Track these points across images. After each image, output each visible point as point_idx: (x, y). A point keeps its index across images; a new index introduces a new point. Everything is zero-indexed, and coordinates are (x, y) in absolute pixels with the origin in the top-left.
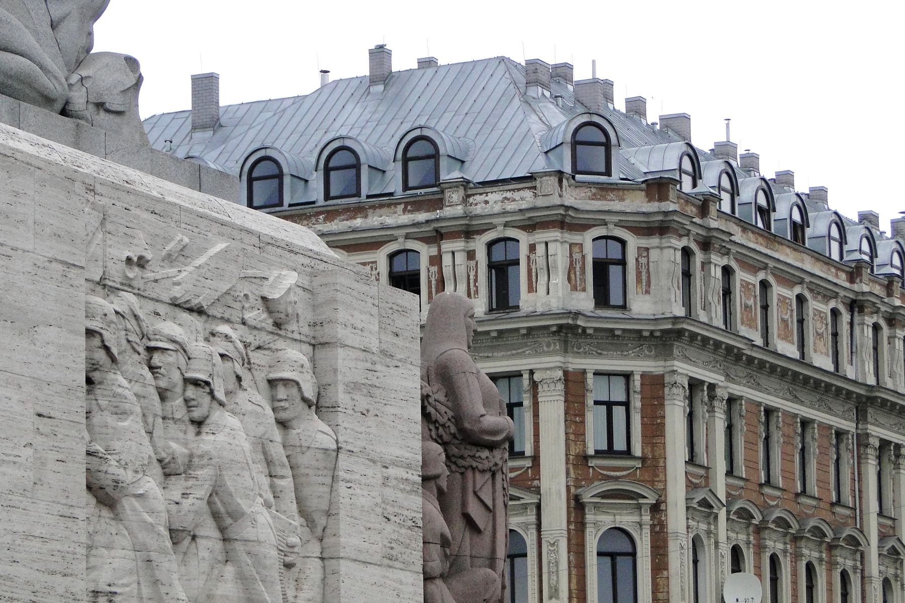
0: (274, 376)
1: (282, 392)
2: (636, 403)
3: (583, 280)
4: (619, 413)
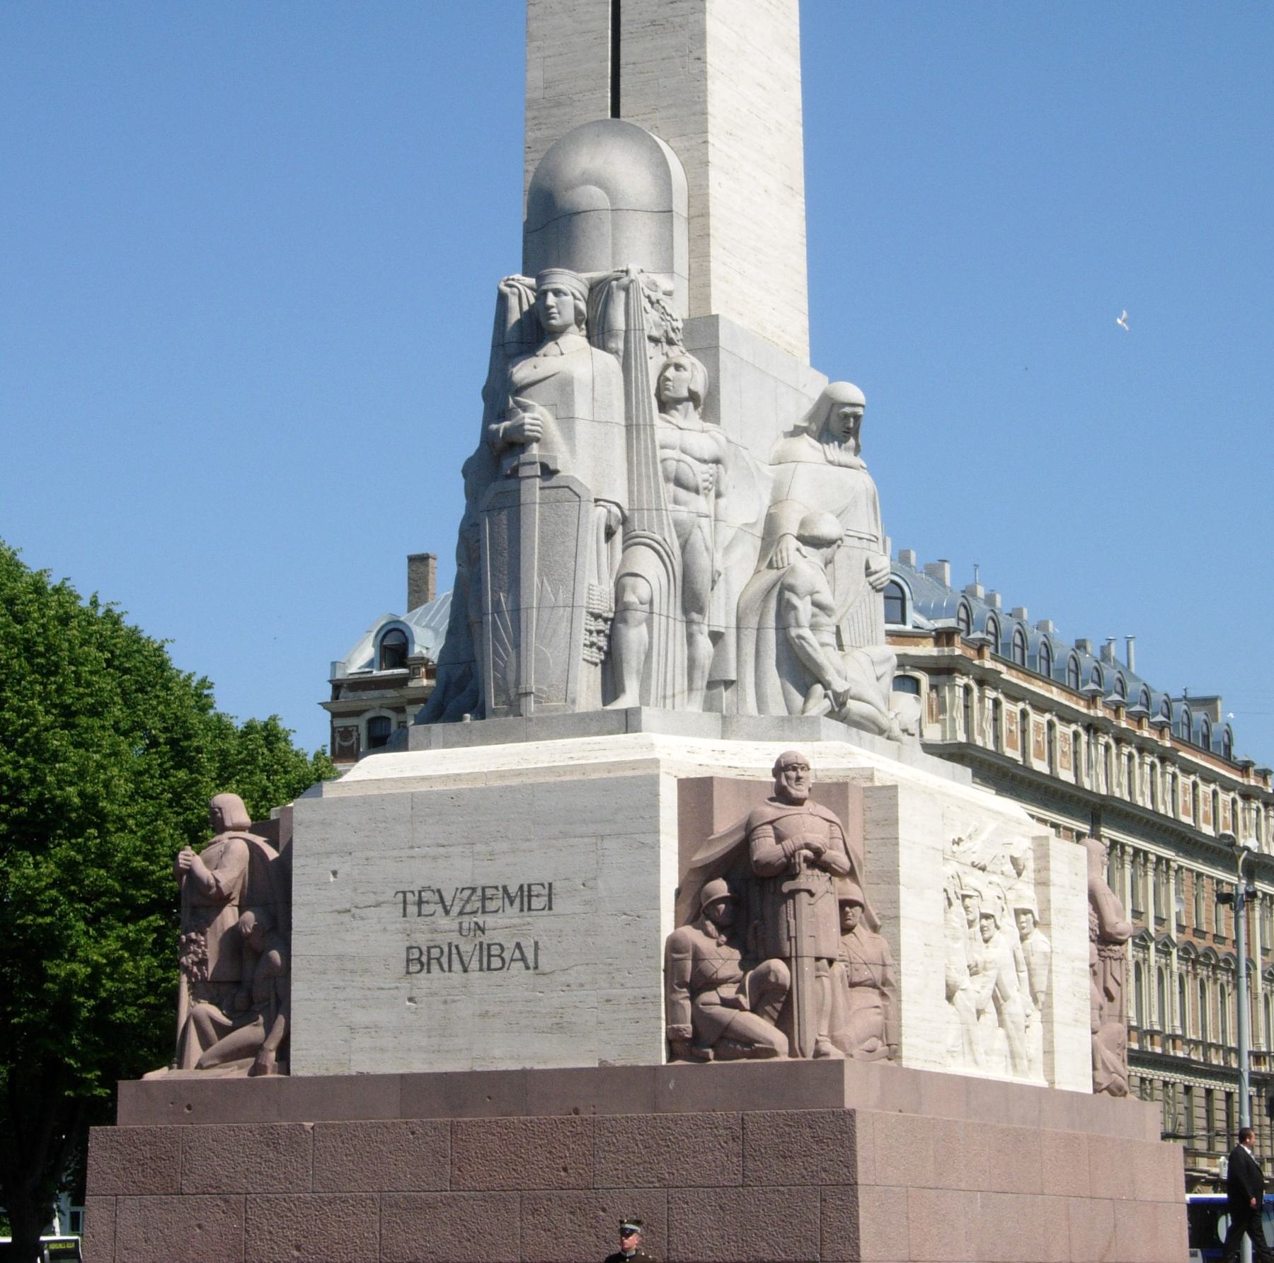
0: (1019, 906)
1: (1023, 918)
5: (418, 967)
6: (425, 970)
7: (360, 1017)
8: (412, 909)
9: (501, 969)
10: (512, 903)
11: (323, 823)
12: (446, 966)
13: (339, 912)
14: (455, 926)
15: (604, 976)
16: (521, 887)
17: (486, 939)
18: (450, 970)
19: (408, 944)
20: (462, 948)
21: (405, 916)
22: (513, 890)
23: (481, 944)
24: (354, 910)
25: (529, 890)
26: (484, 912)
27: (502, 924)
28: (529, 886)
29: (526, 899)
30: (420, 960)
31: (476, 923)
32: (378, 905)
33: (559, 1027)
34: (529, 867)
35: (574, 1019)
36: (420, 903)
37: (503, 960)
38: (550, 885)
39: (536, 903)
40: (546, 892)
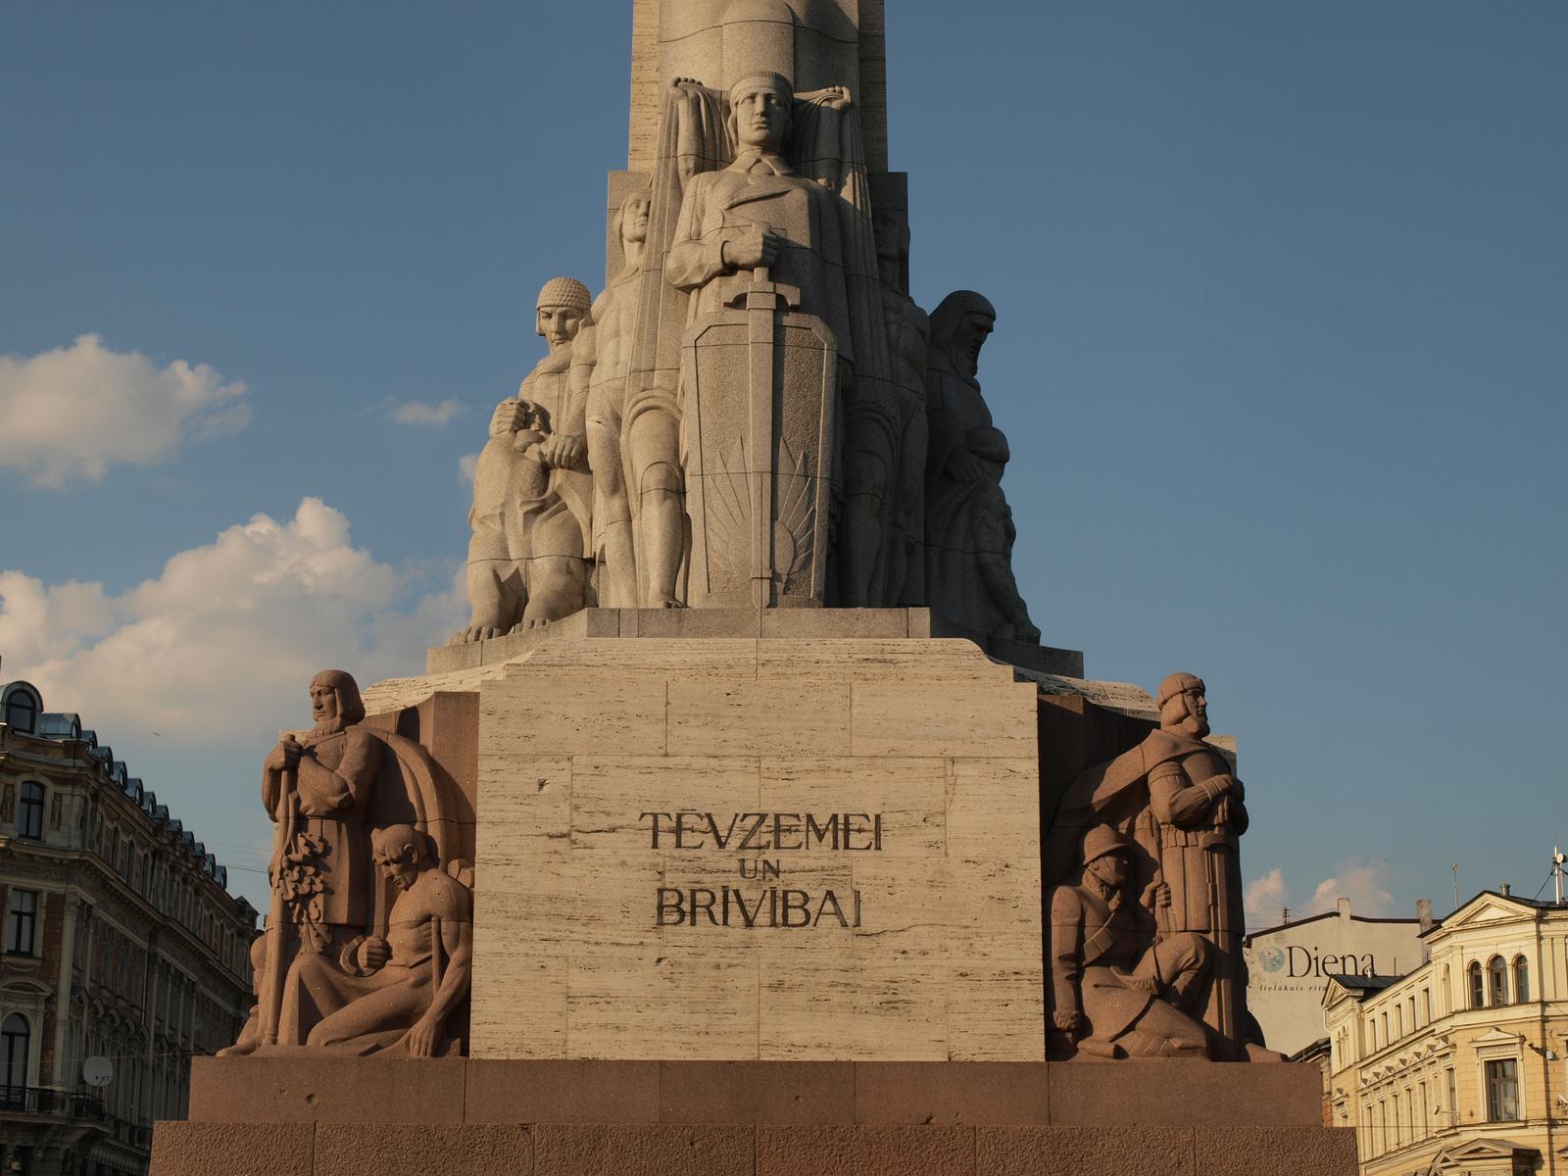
2: (42, 915)
3: (12, 814)
4: (26, 920)
5: (675, 917)
6: (688, 919)
7: (580, 982)
8: (667, 840)
9: (802, 925)
10: (821, 837)
11: (528, 714)
12: (719, 917)
13: (551, 836)
14: (735, 865)
15: (958, 943)
16: (834, 818)
17: (779, 884)
18: (725, 923)
19: (659, 885)
20: (744, 895)
21: (655, 845)
22: (822, 820)
23: (774, 892)
24: (574, 835)
26: (778, 847)
27: (805, 864)
28: (846, 817)
29: (841, 835)
31: (766, 862)
32: (613, 830)
33: (890, 1006)
34: (859, 795)
35: (912, 997)
36: (678, 830)
38: (878, 817)
39: (855, 840)
40: (872, 825)
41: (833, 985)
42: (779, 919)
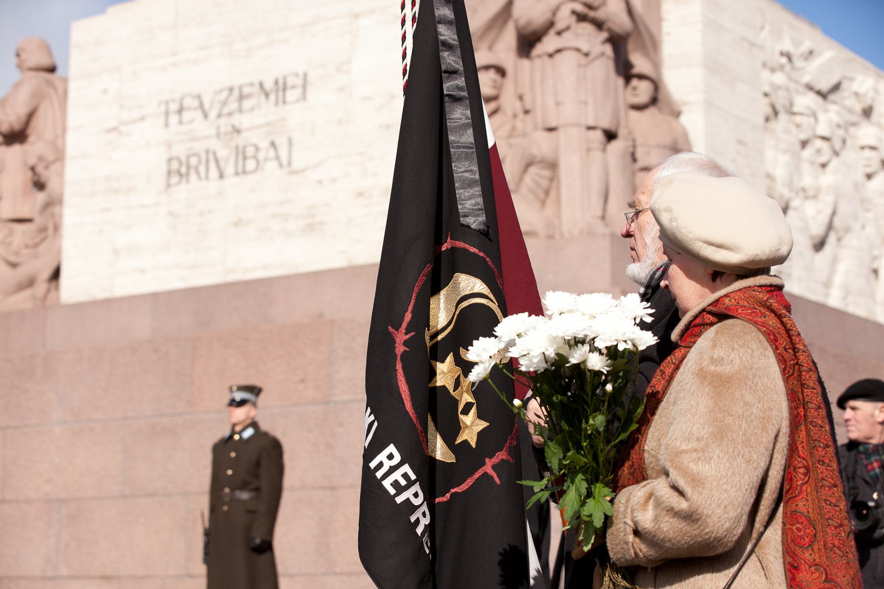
8: (174, 119)
14: (212, 131)
16: (276, 82)
17: (240, 140)
21: (167, 125)
22: (269, 85)
23: (237, 147)
25: (285, 83)
26: (241, 110)
30: (179, 171)
32: (142, 119)
33: (310, 228)
36: (180, 111)
37: (258, 162)
39: (291, 95)
40: (299, 82)
41: (274, 216)
42: (240, 168)
